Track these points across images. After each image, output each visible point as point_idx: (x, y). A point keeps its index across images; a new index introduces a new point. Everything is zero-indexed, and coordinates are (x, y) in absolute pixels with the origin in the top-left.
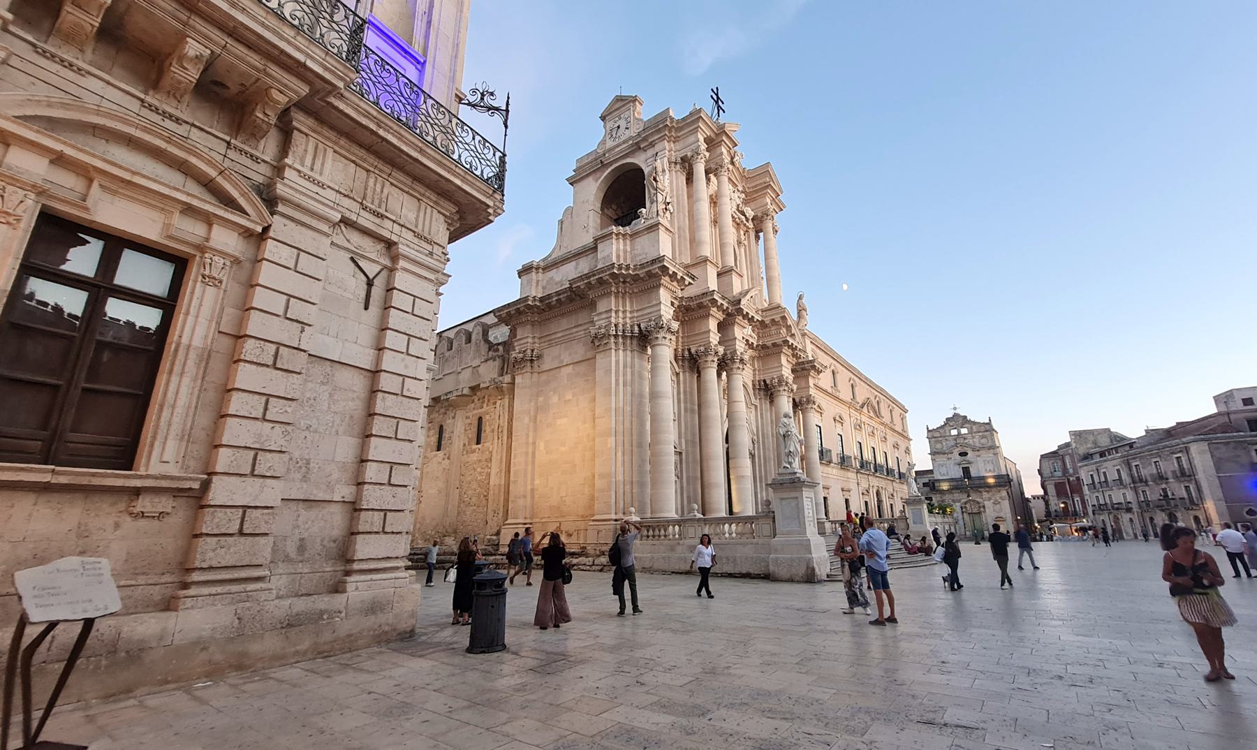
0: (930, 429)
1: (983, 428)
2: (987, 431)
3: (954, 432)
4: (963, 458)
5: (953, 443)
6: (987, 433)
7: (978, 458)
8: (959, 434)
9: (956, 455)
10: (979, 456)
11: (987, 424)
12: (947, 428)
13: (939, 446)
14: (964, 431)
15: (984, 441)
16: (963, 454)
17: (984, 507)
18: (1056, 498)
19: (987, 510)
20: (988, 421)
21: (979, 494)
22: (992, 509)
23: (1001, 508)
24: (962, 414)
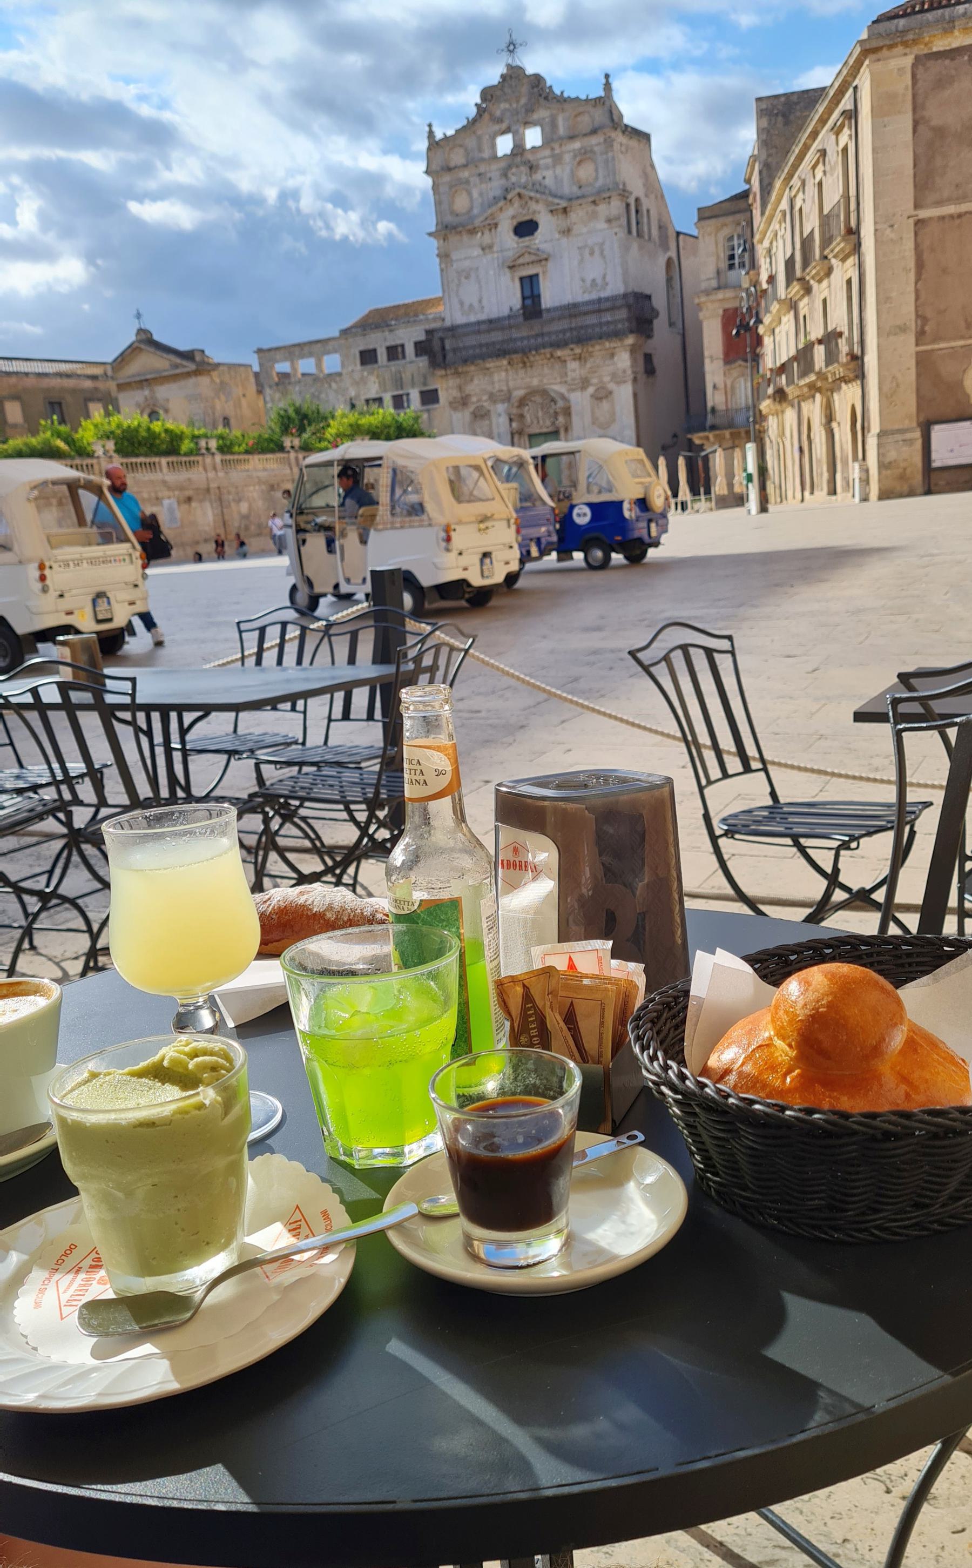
0: (439, 135)
1: (585, 122)
2: (594, 132)
3: (504, 144)
4: (526, 240)
5: (495, 187)
6: (594, 140)
7: (564, 240)
8: (519, 148)
9: (506, 239)
10: (567, 232)
11: (598, 101)
12: (485, 128)
13: (461, 203)
14: (533, 137)
15: (586, 172)
16: (526, 228)
17: (567, 412)
18: (721, 363)
19: (575, 419)
20: (600, 92)
21: (558, 366)
22: (588, 419)
23: (613, 414)
24: (530, 70)
